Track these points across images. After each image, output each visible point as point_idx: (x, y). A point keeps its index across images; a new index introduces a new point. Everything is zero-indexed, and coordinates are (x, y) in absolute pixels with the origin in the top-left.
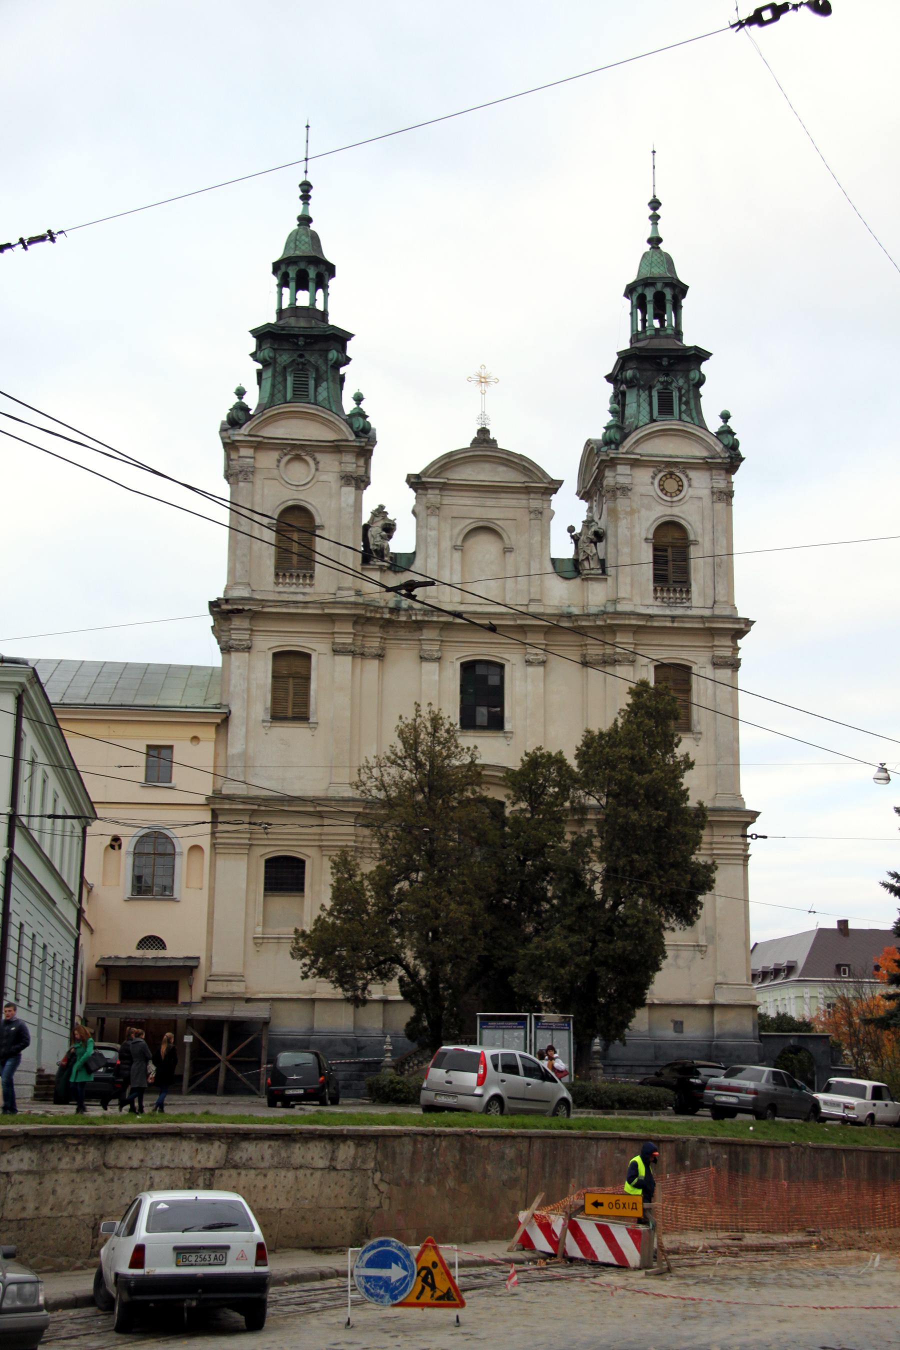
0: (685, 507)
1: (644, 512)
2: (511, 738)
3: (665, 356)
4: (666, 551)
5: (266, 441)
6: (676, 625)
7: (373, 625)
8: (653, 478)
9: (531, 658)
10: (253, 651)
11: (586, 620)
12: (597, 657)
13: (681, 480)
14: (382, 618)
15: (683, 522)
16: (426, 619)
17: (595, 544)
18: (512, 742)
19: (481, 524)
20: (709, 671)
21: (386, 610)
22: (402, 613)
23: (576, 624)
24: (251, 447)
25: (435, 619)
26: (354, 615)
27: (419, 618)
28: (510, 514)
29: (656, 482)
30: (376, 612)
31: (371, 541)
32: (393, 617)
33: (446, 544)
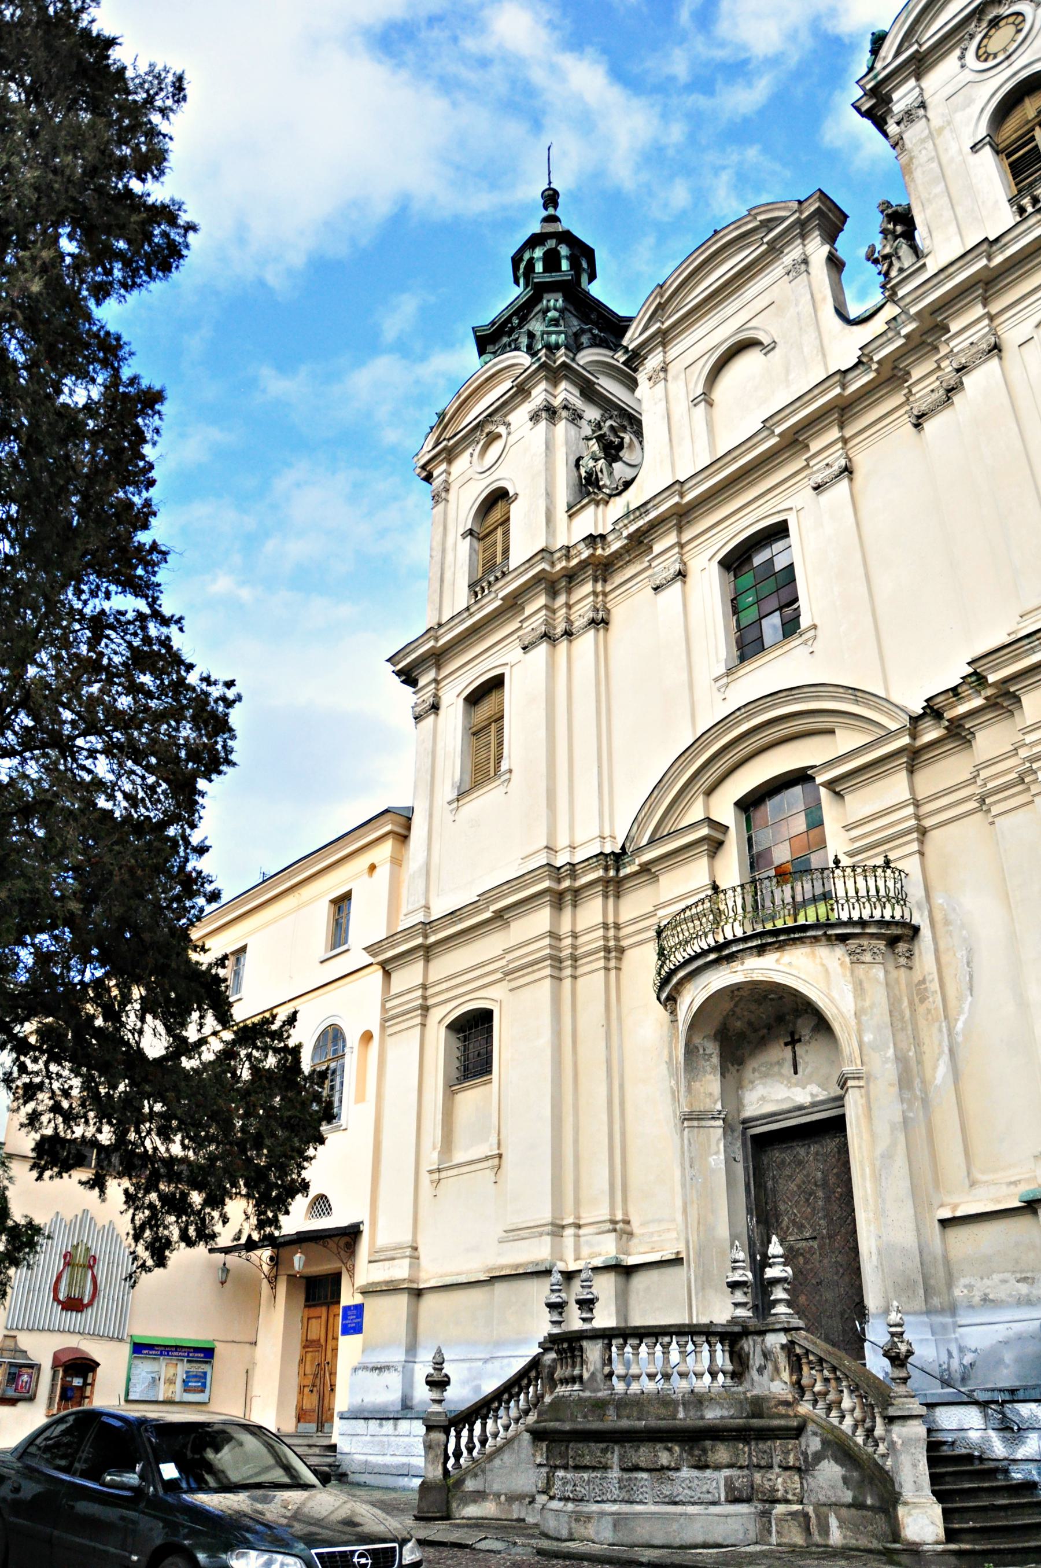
1: (959, 117)
2: (815, 637)
5: (452, 442)
7: (583, 582)
9: (818, 478)
10: (442, 711)
12: (935, 396)
14: (583, 565)
16: (641, 523)
18: (817, 646)
21: (582, 545)
22: (610, 538)
23: (875, 366)
26: (538, 579)
27: (632, 528)
30: (568, 558)
32: (599, 552)
33: (680, 405)
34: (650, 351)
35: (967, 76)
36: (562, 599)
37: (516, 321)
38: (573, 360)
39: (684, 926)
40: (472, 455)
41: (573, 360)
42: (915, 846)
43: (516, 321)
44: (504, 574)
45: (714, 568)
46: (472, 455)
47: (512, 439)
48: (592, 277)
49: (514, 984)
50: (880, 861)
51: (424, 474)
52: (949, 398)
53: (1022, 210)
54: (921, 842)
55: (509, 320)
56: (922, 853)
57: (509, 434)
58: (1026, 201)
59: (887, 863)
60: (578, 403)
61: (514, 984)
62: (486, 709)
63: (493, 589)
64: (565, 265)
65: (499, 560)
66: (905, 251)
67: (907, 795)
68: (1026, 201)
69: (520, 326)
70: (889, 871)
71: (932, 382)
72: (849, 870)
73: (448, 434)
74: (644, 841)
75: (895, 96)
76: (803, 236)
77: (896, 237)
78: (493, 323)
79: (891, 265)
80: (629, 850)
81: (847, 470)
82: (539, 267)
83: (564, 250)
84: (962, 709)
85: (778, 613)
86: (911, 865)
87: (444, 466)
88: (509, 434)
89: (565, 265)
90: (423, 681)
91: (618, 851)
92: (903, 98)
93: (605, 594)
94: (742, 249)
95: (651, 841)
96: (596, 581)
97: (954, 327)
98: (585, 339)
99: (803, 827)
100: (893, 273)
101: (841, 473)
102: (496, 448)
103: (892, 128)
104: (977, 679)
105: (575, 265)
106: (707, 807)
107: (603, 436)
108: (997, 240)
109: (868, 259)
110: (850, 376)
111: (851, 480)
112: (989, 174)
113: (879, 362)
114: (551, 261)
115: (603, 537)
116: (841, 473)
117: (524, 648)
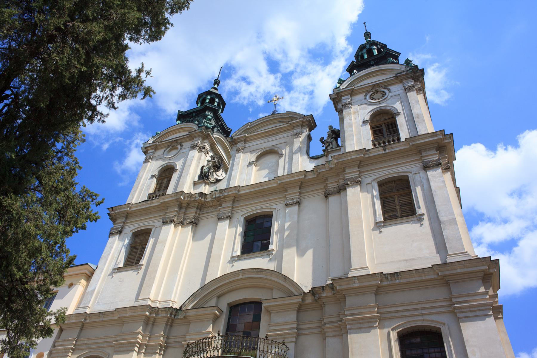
0: (388, 102)
3: (372, 60)
4: (381, 126)
6: (387, 151)
8: (366, 96)
9: (288, 202)
10: (123, 234)
11: (322, 168)
13: (384, 92)
15: (388, 108)
17: (336, 140)
19: (266, 149)
20: (422, 174)
22: (208, 196)
24: (153, 149)
25: (226, 194)
28: (283, 140)
29: (368, 97)
31: (203, 172)
34: (240, 142)
35: (365, 101)
36: (183, 210)
37: (194, 114)
38: (212, 134)
39: (201, 345)
40: (165, 151)
41: (212, 134)
42: (294, 339)
43: (194, 114)
44: (163, 195)
45: (242, 219)
46: (165, 151)
47: (182, 151)
48: (222, 112)
49: (117, 349)
50: (281, 341)
51: (145, 150)
52: (339, 192)
53: (374, 145)
54: (296, 339)
55: (192, 113)
56: (296, 343)
57: (181, 149)
58: (377, 143)
59: (283, 344)
60: (208, 147)
61: (117, 349)
62: (139, 239)
63: (160, 198)
64: (216, 104)
65: (162, 189)
66: (334, 143)
67: (295, 319)
68: (377, 143)
69: (195, 116)
70: (284, 346)
71: (335, 185)
72: (270, 341)
73: (158, 140)
74: (190, 307)
75: (343, 98)
76: (302, 126)
77: (332, 138)
78: (186, 112)
79: (329, 145)
80: (183, 309)
81: (298, 203)
82: (207, 101)
83: (217, 100)
84: (324, 295)
85: (260, 242)
86: (291, 346)
87: (153, 150)
88: (181, 149)
89: (216, 104)
90: (119, 221)
91: (178, 308)
92: (346, 99)
93: (199, 214)
94: (280, 122)
95: (192, 309)
96: (197, 208)
97: (347, 171)
98: (215, 129)
99: (251, 320)
100: (329, 148)
101: (296, 203)
102: (174, 152)
103: (340, 106)
104: (332, 287)
105: (219, 105)
106: (217, 302)
107: (215, 162)
108: (368, 150)
109: (320, 141)
110: (308, 173)
111: (299, 206)
112: (367, 131)
113: (320, 173)
114: (212, 101)
115: (205, 194)
116: (296, 203)
117: (163, 223)
